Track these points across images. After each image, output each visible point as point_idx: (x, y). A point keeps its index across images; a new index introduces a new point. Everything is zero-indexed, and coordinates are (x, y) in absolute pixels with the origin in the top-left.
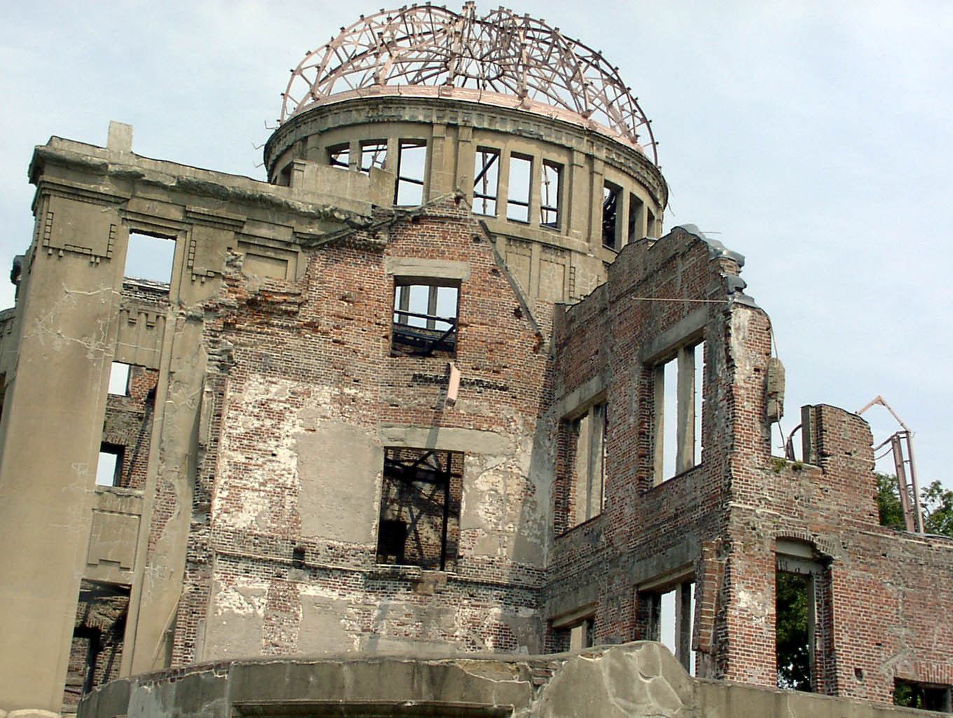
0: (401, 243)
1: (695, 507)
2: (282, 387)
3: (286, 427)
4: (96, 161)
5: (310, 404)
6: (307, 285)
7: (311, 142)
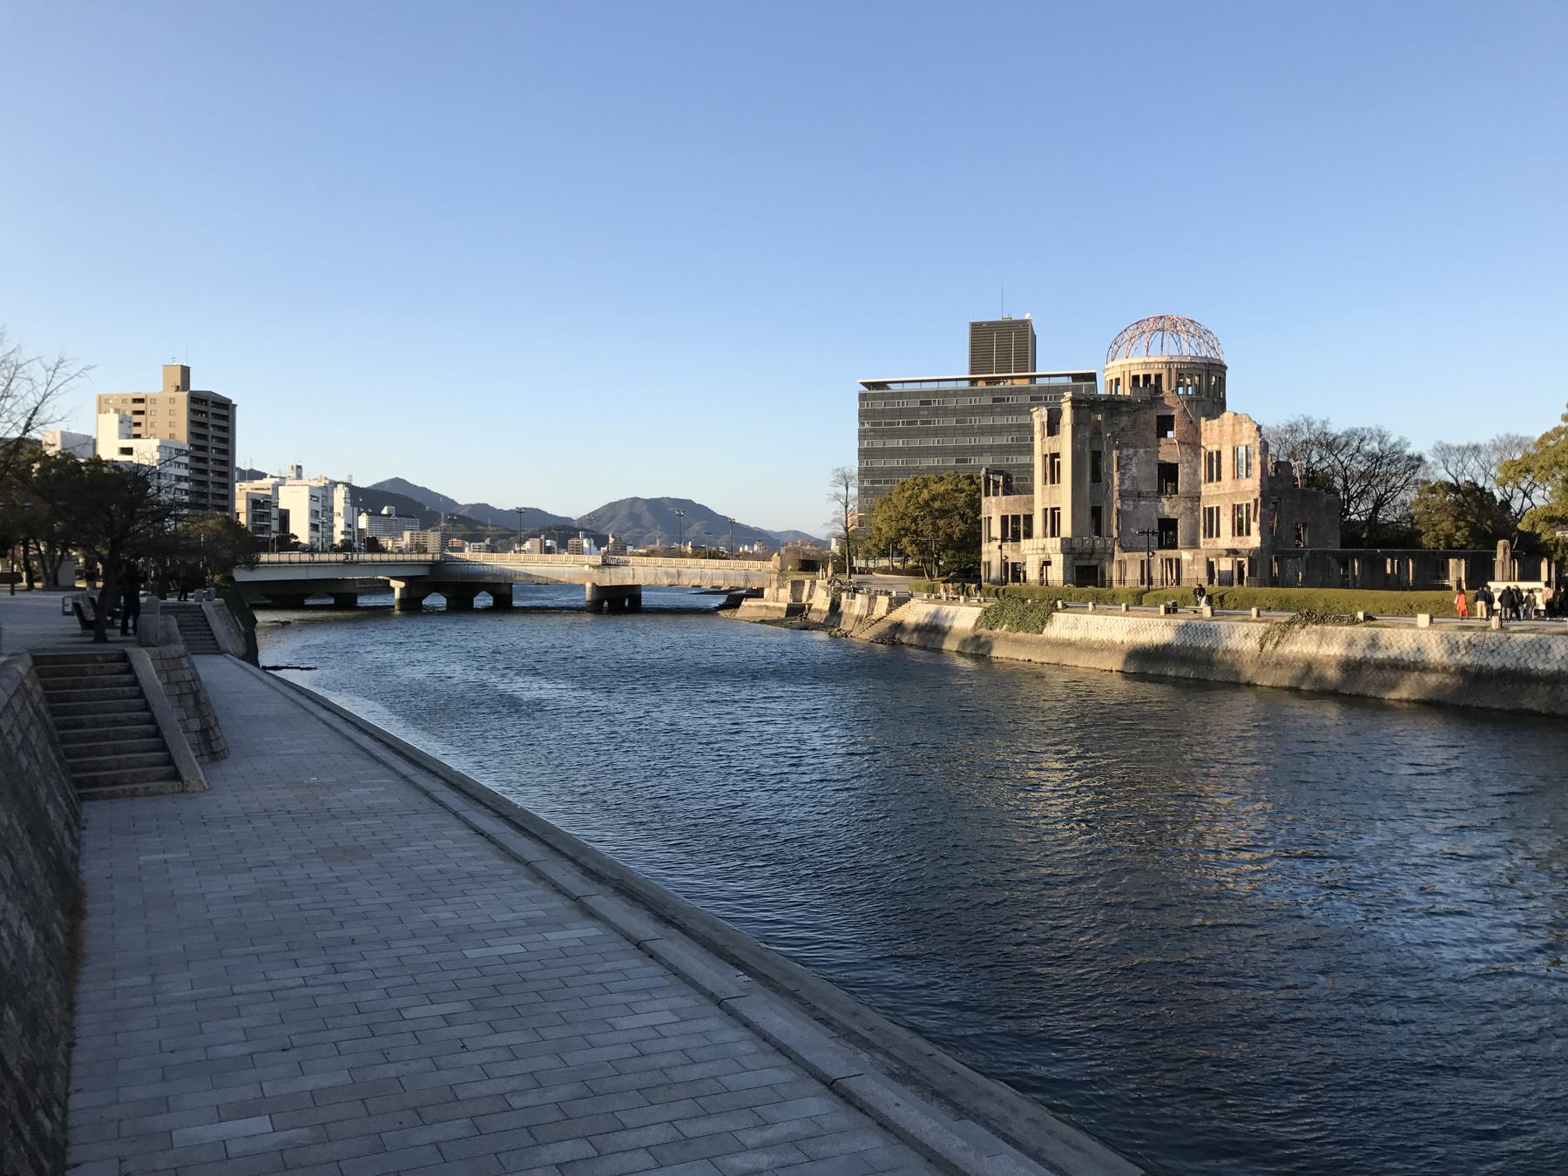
2: (1131, 451)
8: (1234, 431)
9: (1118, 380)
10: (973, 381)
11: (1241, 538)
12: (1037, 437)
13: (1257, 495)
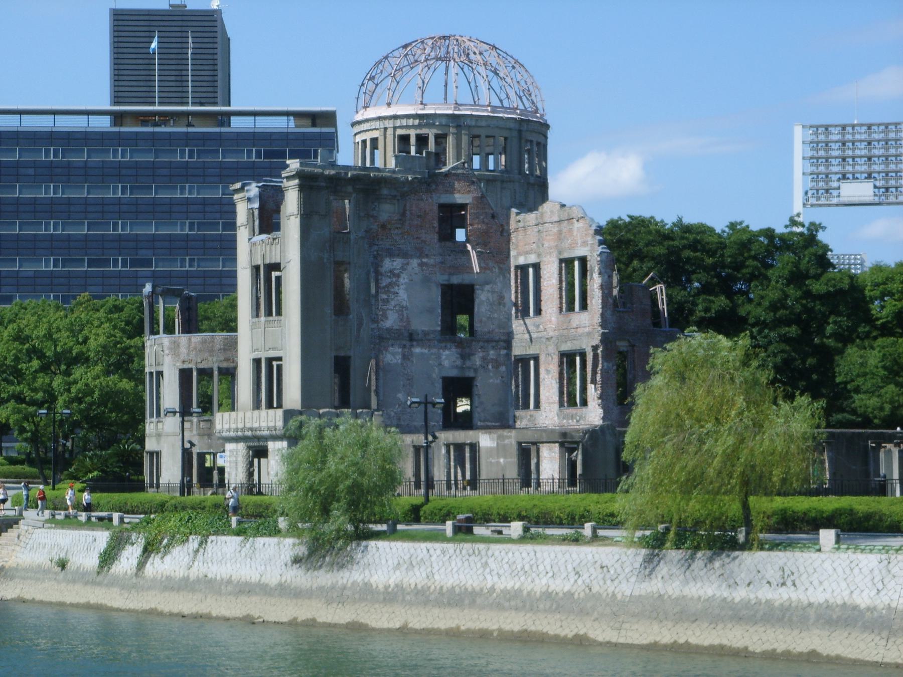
0: (441, 187)
1: (585, 327)
2: (398, 263)
3: (401, 280)
4: (320, 171)
5: (409, 268)
6: (403, 214)
7: (390, 132)
8: (560, 232)
9: (374, 141)
10: (118, 118)
11: (572, 411)
12: (243, 235)
13: (596, 340)
